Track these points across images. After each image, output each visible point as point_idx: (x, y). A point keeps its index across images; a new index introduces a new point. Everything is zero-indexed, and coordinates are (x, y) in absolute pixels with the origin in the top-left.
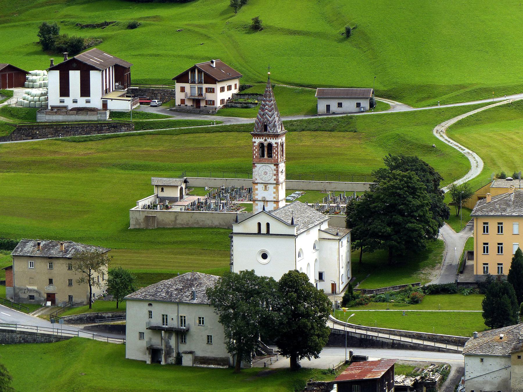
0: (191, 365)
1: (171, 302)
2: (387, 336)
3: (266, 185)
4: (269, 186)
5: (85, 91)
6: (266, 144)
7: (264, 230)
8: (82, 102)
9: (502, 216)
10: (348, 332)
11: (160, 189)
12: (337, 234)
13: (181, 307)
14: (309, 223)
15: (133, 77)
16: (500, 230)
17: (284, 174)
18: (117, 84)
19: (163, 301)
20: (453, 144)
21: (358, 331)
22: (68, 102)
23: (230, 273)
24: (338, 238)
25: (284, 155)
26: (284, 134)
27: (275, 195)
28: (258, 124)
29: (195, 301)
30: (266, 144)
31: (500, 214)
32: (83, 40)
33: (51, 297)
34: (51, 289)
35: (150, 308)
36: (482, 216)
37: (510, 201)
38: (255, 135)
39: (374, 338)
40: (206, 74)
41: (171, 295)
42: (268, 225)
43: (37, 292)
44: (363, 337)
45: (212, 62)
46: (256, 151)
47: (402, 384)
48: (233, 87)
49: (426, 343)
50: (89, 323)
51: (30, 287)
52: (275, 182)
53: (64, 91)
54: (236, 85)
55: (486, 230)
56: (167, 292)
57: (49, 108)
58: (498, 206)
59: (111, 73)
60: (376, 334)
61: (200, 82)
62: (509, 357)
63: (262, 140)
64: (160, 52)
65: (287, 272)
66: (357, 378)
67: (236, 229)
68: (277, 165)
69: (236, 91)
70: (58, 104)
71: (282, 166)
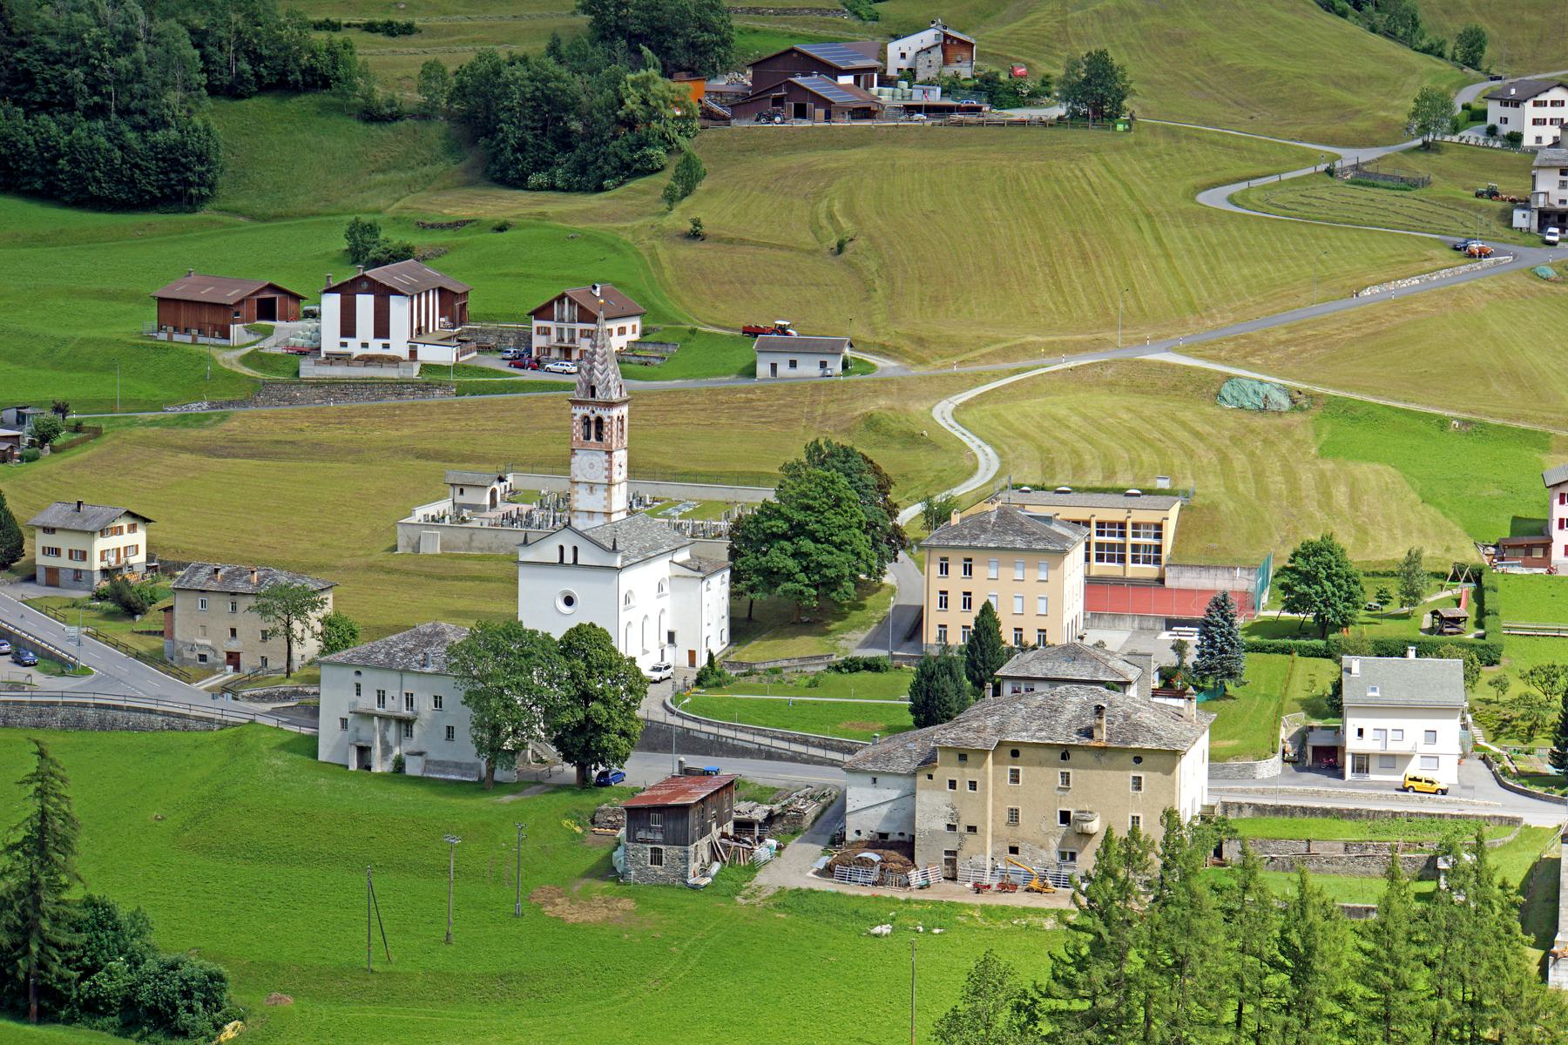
0: (420, 774)
1: (390, 669)
2: (749, 737)
3: (592, 487)
4: (596, 487)
5: (382, 330)
6: (592, 418)
7: (569, 559)
8: (376, 347)
9: (970, 547)
10: (688, 730)
11: (458, 490)
12: (699, 570)
13: (407, 679)
14: (652, 548)
15: (471, 308)
16: (968, 570)
17: (625, 468)
18: (443, 320)
19: (380, 667)
20: (957, 432)
21: (705, 728)
22: (354, 347)
23: (514, 630)
24: (701, 575)
25: (626, 438)
26: (625, 402)
27: (605, 503)
28: (580, 384)
29: (428, 670)
30: (592, 418)
31: (967, 544)
32: (413, 247)
33: (233, 658)
34: (234, 646)
35: (358, 680)
36: (938, 547)
37: (989, 522)
38: (575, 403)
39: (730, 741)
40: (580, 307)
41: (394, 659)
42: (575, 549)
43: (211, 649)
44: (712, 737)
45: (595, 288)
46: (578, 430)
47: (746, 816)
48: (629, 330)
49: (813, 751)
50: (280, 700)
51: (200, 641)
52: (606, 481)
53: (348, 329)
54: (634, 327)
55: (944, 569)
56: (388, 654)
57: (323, 355)
58: (966, 532)
59: (434, 300)
60: (731, 734)
61: (572, 321)
62: (914, 775)
63: (587, 411)
64: (532, 271)
65: (574, 626)
66: (659, 802)
67: (526, 555)
68: (609, 453)
69: (636, 337)
70: (338, 349)
71: (621, 457)
